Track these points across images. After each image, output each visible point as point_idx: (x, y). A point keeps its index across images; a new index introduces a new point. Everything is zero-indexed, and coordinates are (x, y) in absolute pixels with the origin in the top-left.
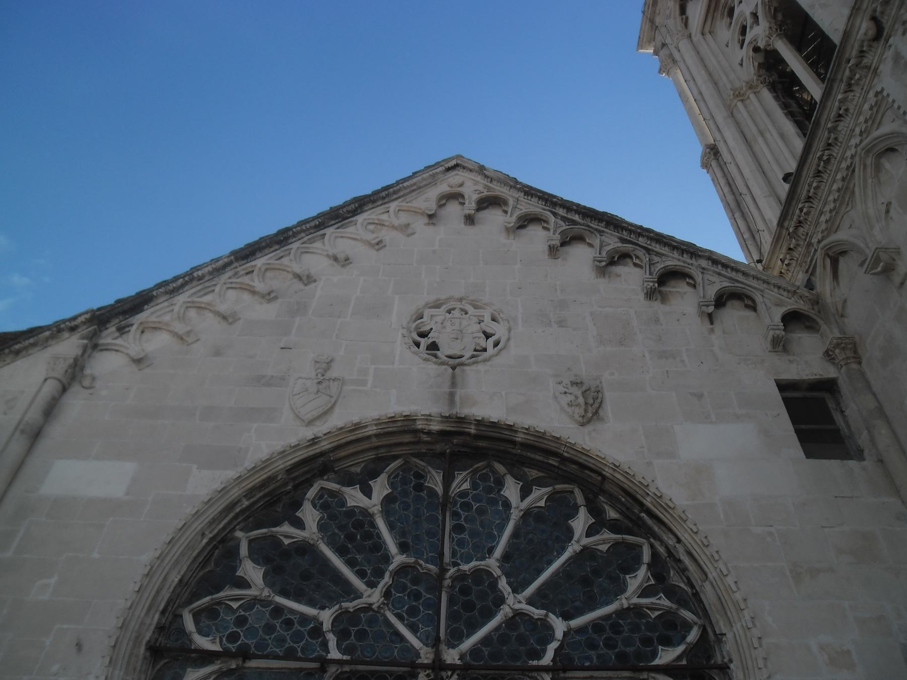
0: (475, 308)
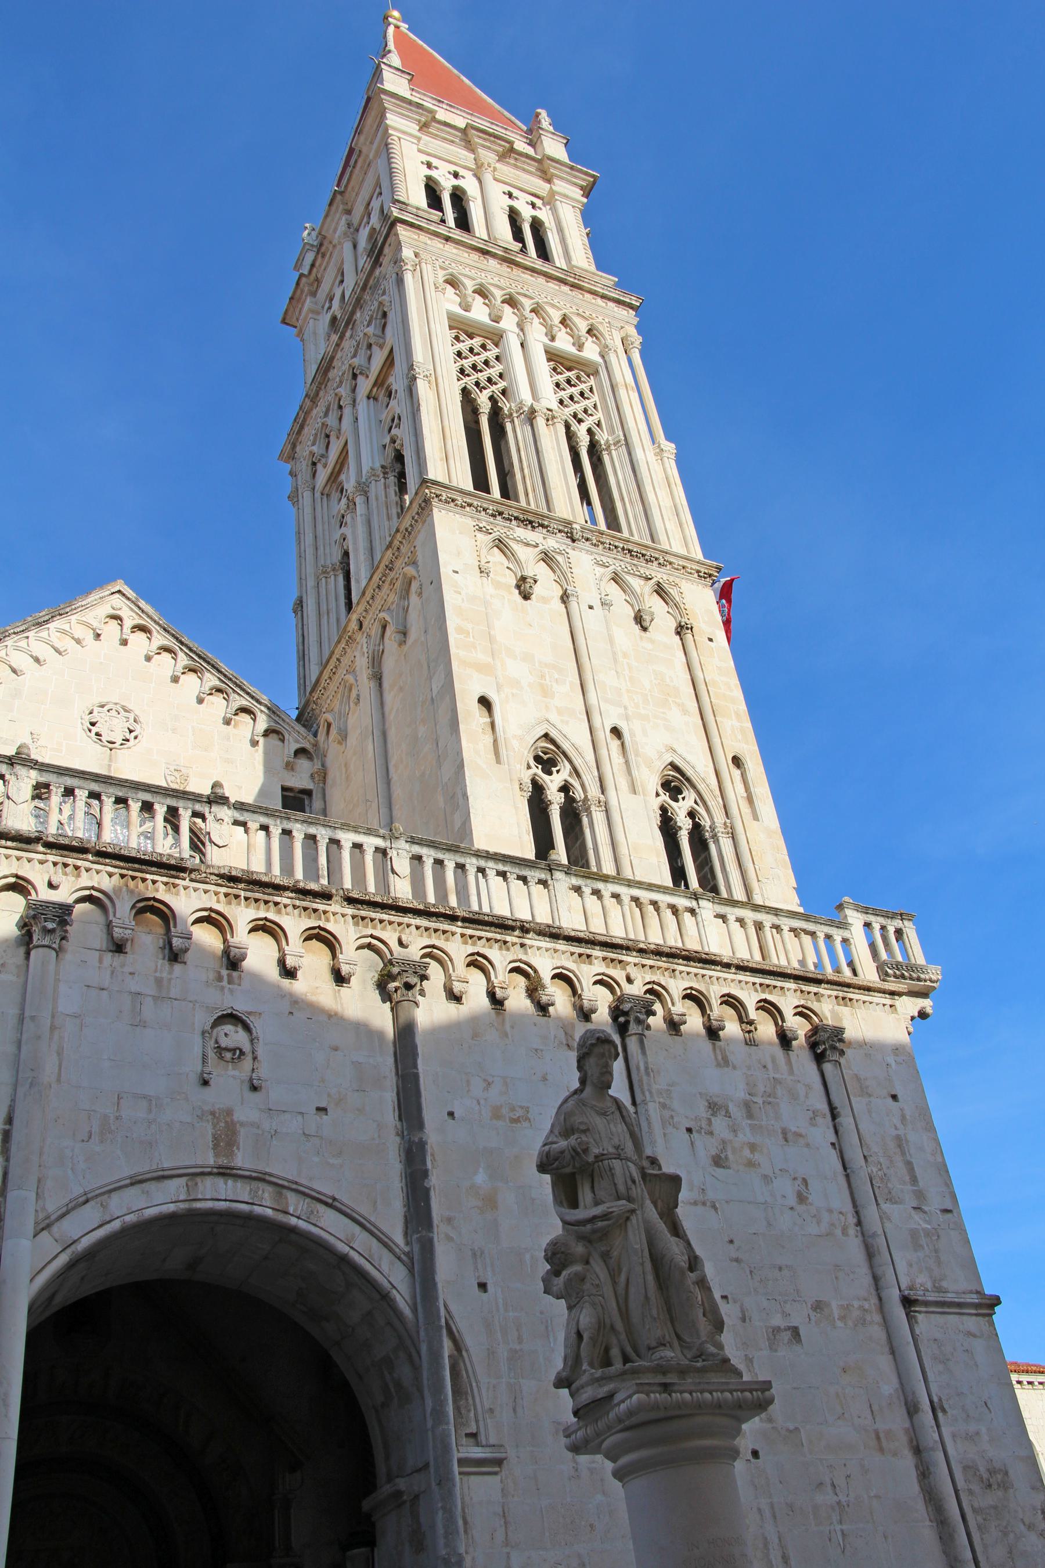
0: (126, 711)
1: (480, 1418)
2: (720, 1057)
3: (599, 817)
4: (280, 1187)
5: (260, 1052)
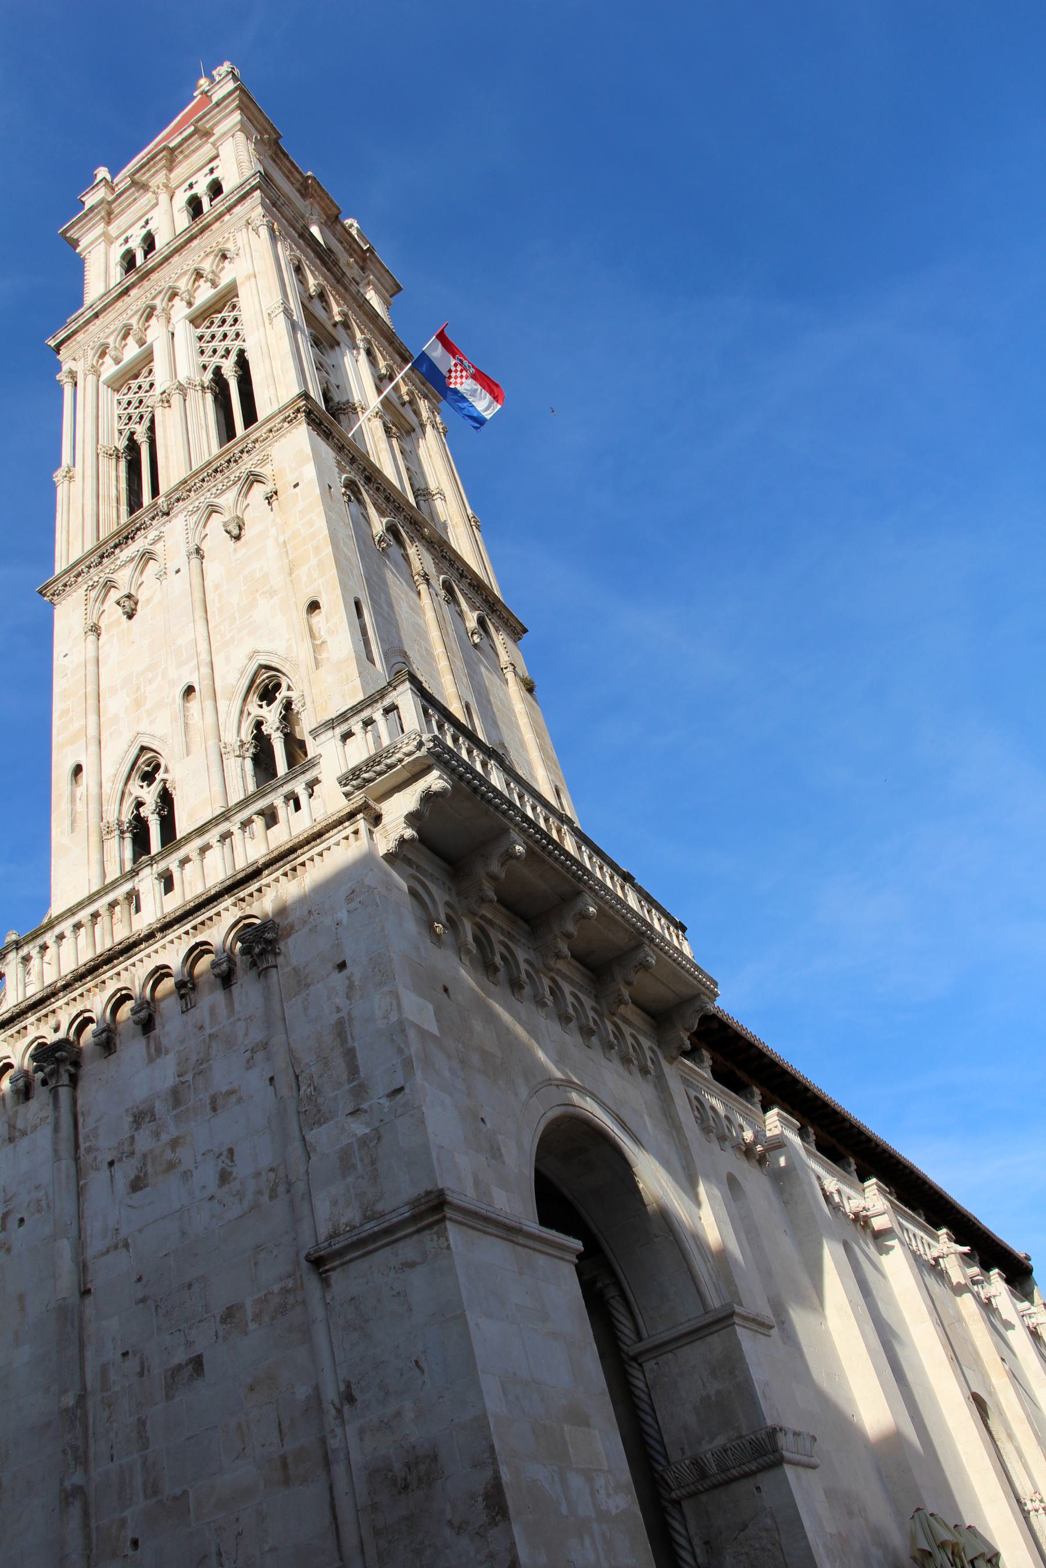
2: (152, 1050)
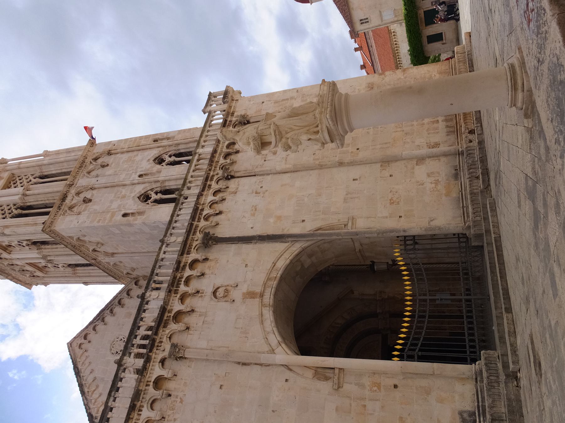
1: (341, 223)
3: (167, 184)
4: (269, 279)
5: (226, 284)
